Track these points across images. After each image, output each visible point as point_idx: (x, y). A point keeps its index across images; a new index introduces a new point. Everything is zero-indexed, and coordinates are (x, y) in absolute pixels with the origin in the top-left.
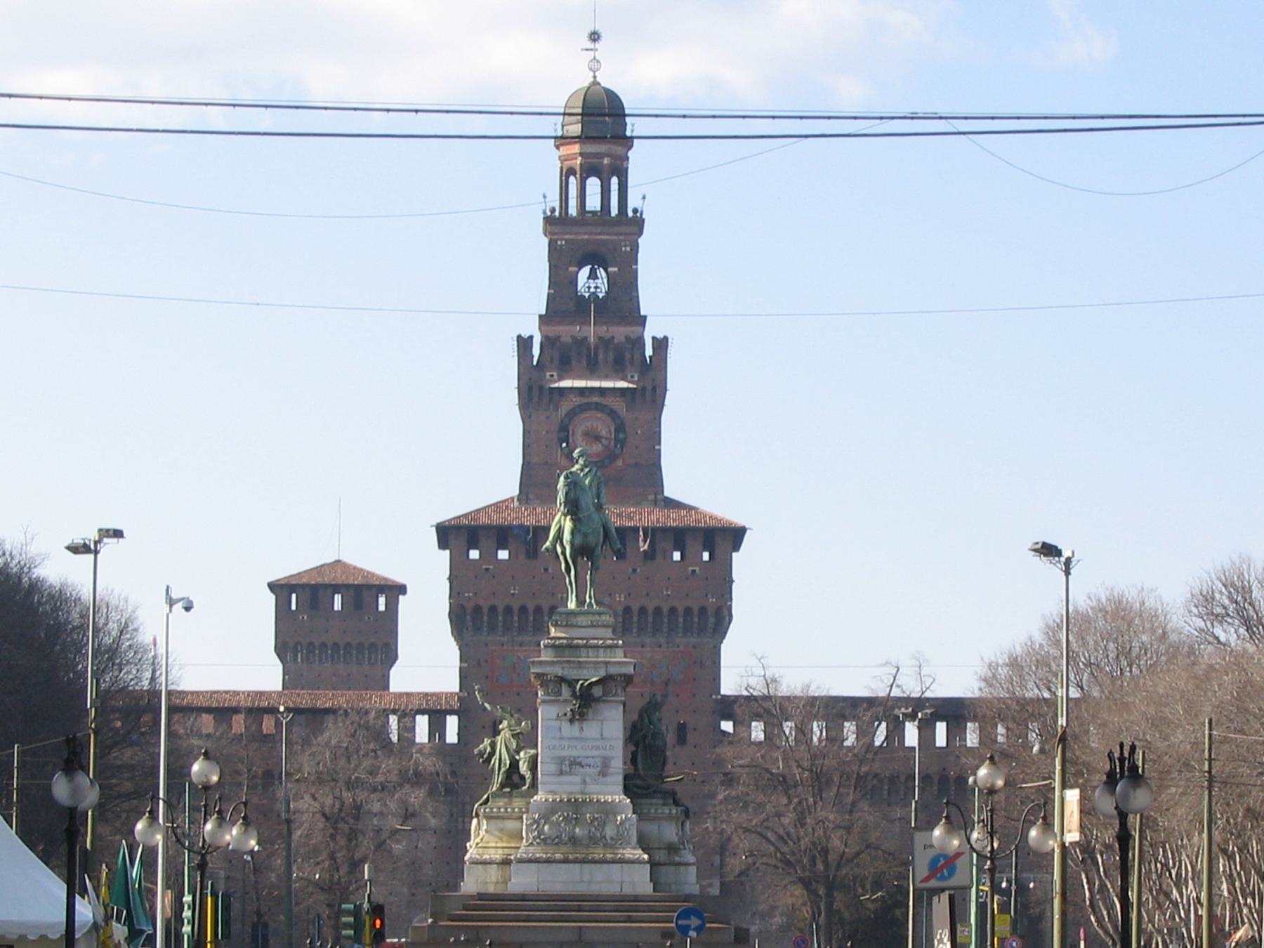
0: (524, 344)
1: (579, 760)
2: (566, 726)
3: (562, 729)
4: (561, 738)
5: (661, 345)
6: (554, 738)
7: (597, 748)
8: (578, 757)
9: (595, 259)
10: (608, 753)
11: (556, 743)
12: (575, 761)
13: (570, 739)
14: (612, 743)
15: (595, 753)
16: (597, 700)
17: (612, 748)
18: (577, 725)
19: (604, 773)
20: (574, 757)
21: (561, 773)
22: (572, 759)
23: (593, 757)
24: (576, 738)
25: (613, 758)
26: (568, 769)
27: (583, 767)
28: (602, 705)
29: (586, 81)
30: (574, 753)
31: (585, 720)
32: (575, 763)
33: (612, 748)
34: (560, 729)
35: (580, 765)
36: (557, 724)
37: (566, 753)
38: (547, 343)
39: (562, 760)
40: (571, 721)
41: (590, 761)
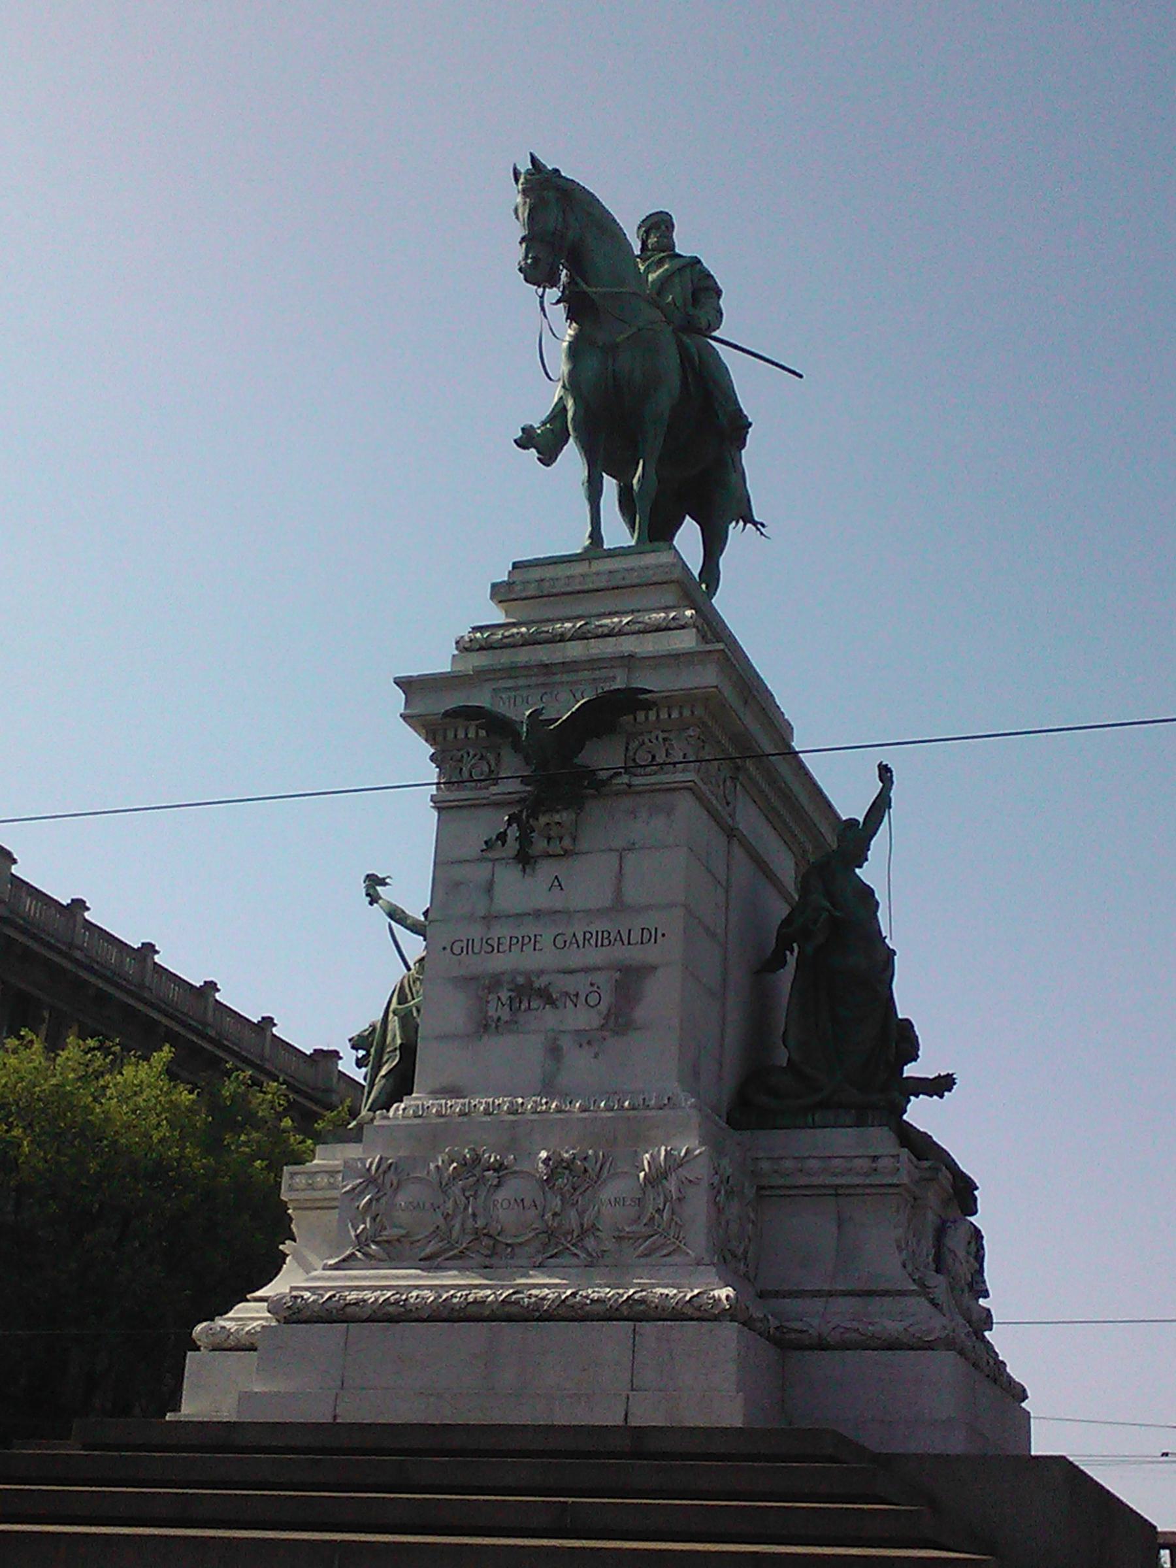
1: (539, 983)
3: (497, 888)
4: (490, 919)
7: (605, 940)
8: (542, 972)
10: (635, 954)
11: (476, 931)
12: (531, 983)
13: (519, 917)
14: (651, 920)
15: (594, 956)
17: (650, 936)
18: (546, 870)
20: (527, 975)
21: (485, 1026)
22: (521, 980)
23: (586, 970)
24: (537, 914)
25: (653, 968)
26: (505, 1015)
27: (550, 1001)
28: (627, 803)
31: (567, 853)
33: (650, 936)
34: (489, 888)
35: (547, 997)
36: (481, 872)
37: (500, 963)
39: (495, 982)
40: (525, 859)
41: (579, 984)
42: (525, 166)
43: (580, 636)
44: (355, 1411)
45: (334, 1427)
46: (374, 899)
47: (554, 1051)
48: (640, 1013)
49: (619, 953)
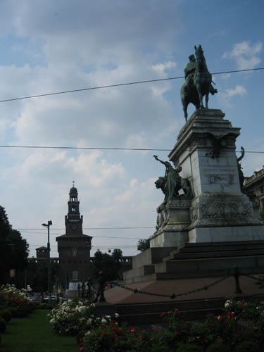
0: (66, 216)
2: (210, 160)
5: (82, 216)
6: (206, 166)
7: (226, 170)
9: (74, 208)
10: (232, 173)
11: (206, 168)
16: (225, 147)
17: (234, 170)
19: (231, 183)
21: (211, 183)
29: (72, 187)
30: (216, 173)
32: (217, 178)
33: (234, 170)
34: (208, 161)
36: (206, 158)
37: (212, 173)
38: (69, 217)
39: (211, 176)
40: (213, 157)
41: (224, 177)
42: (197, 46)
43: (215, 123)
44: (216, 240)
45: (212, 243)
46: (158, 160)
47: (222, 187)
48: (234, 182)
49: (229, 173)
